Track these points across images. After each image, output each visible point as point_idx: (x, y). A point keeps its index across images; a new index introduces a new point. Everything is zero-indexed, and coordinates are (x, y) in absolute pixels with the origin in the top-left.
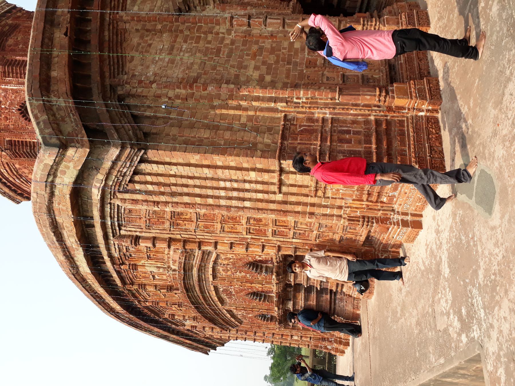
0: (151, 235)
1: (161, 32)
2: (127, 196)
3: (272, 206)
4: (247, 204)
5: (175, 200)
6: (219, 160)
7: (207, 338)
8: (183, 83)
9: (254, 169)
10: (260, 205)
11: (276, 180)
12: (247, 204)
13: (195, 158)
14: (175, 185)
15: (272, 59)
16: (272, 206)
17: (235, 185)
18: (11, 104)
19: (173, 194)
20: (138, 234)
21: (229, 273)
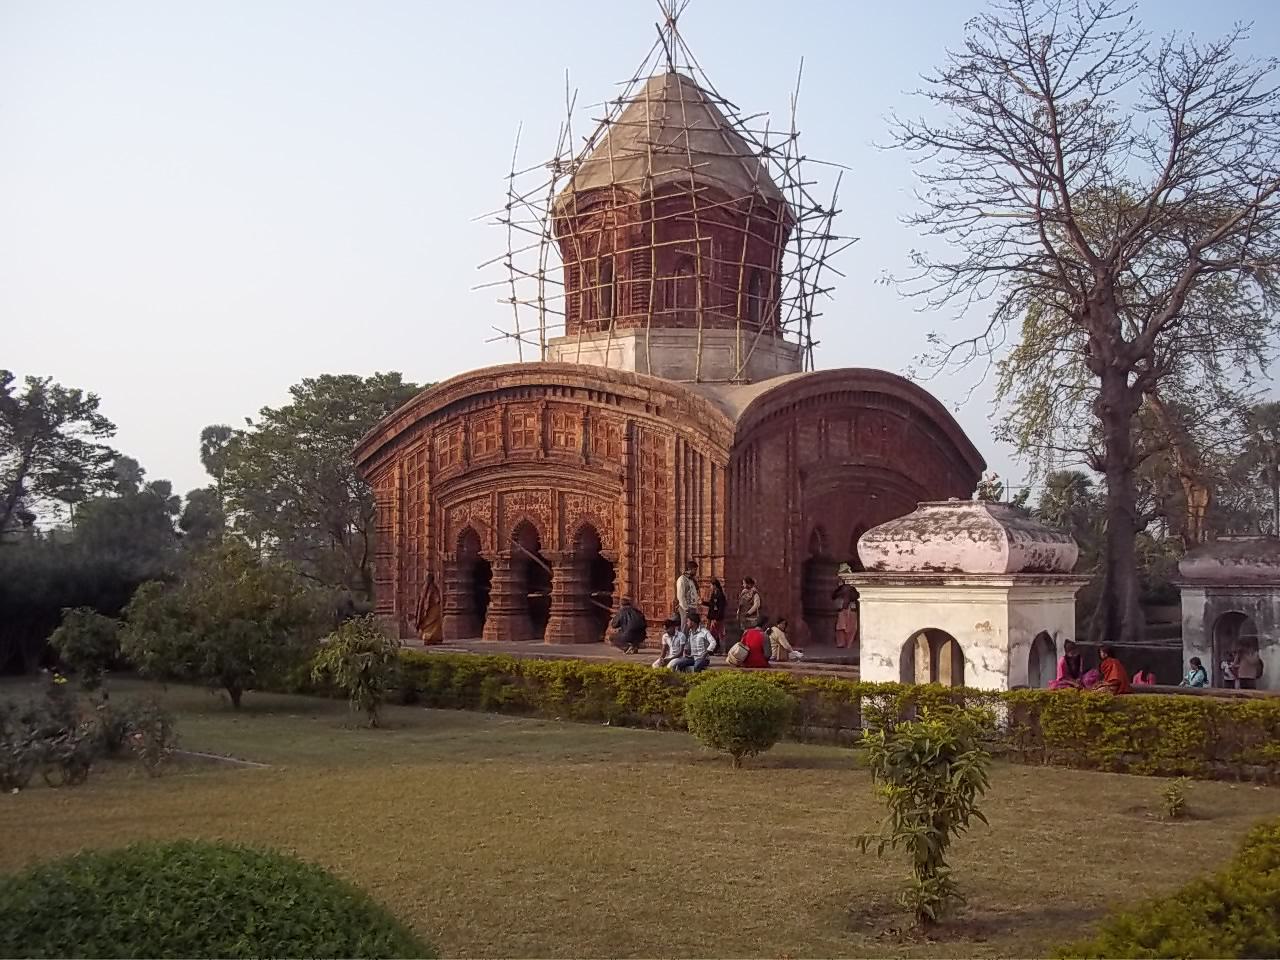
0: (635, 453)
1: (788, 461)
2: (682, 446)
3: (683, 552)
4: (683, 534)
5: (682, 481)
6: (719, 516)
7: (392, 457)
8: (759, 485)
9: (713, 540)
10: (683, 543)
11: (704, 553)
12: (683, 534)
13: (720, 499)
14: (694, 483)
15: (774, 544)
16: (683, 552)
17: (698, 525)
19: (686, 480)
20: (634, 440)
21: (572, 507)
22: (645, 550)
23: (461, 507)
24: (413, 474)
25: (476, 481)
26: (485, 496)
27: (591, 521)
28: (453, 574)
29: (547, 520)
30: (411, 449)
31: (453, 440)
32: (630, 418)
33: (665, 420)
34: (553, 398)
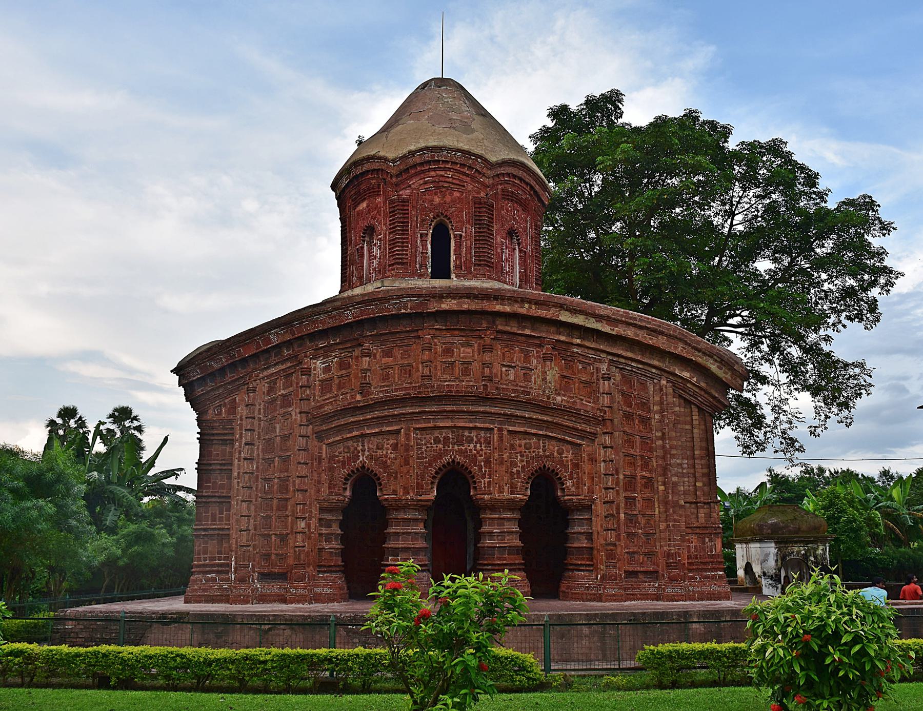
18: (517, 222)
22: (629, 494)
23: (350, 443)
24: (273, 401)
25: (377, 414)
26: (398, 432)
27: (549, 464)
28: (328, 524)
29: (488, 462)
30: (272, 370)
31: (342, 365)
32: (610, 357)
33: (656, 363)
34: (508, 329)
